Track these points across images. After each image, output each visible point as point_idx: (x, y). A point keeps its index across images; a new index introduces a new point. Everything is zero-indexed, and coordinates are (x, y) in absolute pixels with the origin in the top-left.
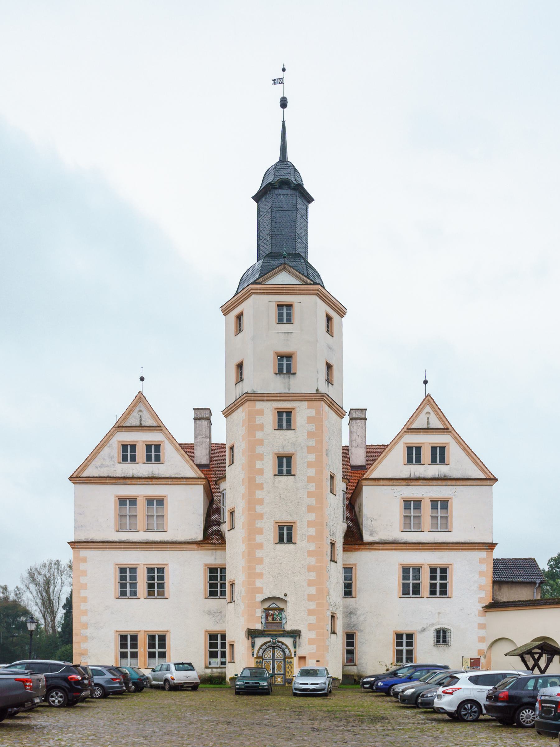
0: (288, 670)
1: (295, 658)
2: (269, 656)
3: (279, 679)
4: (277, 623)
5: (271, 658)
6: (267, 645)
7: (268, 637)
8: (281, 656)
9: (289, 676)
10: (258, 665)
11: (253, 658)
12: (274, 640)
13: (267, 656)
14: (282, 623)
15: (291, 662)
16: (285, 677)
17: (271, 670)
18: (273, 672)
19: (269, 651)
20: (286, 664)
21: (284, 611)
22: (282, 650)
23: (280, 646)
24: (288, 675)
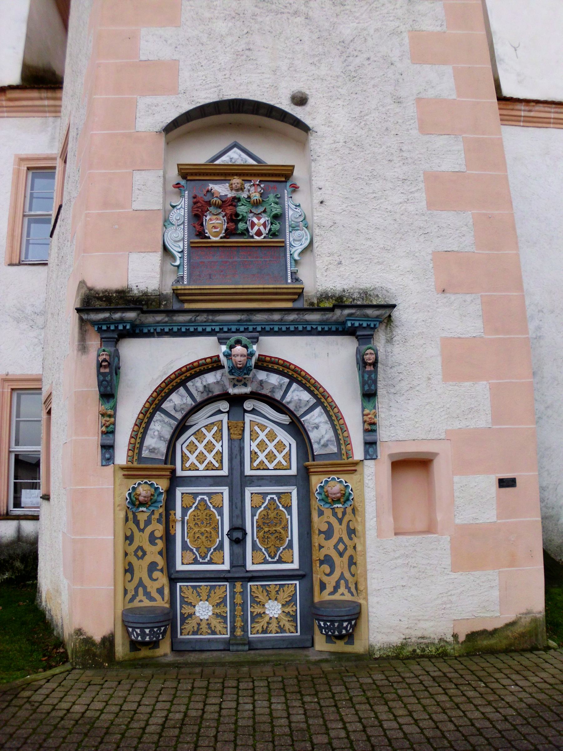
0: (329, 548)
1: (369, 467)
2: (210, 457)
4: (260, 246)
5: (225, 472)
7: (204, 333)
8: (280, 457)
9: (336, 588)
10: (142, 518)
11: (109, 469)
12: (239, 349)
13: (201, 458)
14: (282, 247)
16: (308, 592)
17: (221, 547)
19: (208, 427)
20: (315, 504)
21: (295, 188)
22: (285, 419)
23: (278, 396)
24: (331, 582)
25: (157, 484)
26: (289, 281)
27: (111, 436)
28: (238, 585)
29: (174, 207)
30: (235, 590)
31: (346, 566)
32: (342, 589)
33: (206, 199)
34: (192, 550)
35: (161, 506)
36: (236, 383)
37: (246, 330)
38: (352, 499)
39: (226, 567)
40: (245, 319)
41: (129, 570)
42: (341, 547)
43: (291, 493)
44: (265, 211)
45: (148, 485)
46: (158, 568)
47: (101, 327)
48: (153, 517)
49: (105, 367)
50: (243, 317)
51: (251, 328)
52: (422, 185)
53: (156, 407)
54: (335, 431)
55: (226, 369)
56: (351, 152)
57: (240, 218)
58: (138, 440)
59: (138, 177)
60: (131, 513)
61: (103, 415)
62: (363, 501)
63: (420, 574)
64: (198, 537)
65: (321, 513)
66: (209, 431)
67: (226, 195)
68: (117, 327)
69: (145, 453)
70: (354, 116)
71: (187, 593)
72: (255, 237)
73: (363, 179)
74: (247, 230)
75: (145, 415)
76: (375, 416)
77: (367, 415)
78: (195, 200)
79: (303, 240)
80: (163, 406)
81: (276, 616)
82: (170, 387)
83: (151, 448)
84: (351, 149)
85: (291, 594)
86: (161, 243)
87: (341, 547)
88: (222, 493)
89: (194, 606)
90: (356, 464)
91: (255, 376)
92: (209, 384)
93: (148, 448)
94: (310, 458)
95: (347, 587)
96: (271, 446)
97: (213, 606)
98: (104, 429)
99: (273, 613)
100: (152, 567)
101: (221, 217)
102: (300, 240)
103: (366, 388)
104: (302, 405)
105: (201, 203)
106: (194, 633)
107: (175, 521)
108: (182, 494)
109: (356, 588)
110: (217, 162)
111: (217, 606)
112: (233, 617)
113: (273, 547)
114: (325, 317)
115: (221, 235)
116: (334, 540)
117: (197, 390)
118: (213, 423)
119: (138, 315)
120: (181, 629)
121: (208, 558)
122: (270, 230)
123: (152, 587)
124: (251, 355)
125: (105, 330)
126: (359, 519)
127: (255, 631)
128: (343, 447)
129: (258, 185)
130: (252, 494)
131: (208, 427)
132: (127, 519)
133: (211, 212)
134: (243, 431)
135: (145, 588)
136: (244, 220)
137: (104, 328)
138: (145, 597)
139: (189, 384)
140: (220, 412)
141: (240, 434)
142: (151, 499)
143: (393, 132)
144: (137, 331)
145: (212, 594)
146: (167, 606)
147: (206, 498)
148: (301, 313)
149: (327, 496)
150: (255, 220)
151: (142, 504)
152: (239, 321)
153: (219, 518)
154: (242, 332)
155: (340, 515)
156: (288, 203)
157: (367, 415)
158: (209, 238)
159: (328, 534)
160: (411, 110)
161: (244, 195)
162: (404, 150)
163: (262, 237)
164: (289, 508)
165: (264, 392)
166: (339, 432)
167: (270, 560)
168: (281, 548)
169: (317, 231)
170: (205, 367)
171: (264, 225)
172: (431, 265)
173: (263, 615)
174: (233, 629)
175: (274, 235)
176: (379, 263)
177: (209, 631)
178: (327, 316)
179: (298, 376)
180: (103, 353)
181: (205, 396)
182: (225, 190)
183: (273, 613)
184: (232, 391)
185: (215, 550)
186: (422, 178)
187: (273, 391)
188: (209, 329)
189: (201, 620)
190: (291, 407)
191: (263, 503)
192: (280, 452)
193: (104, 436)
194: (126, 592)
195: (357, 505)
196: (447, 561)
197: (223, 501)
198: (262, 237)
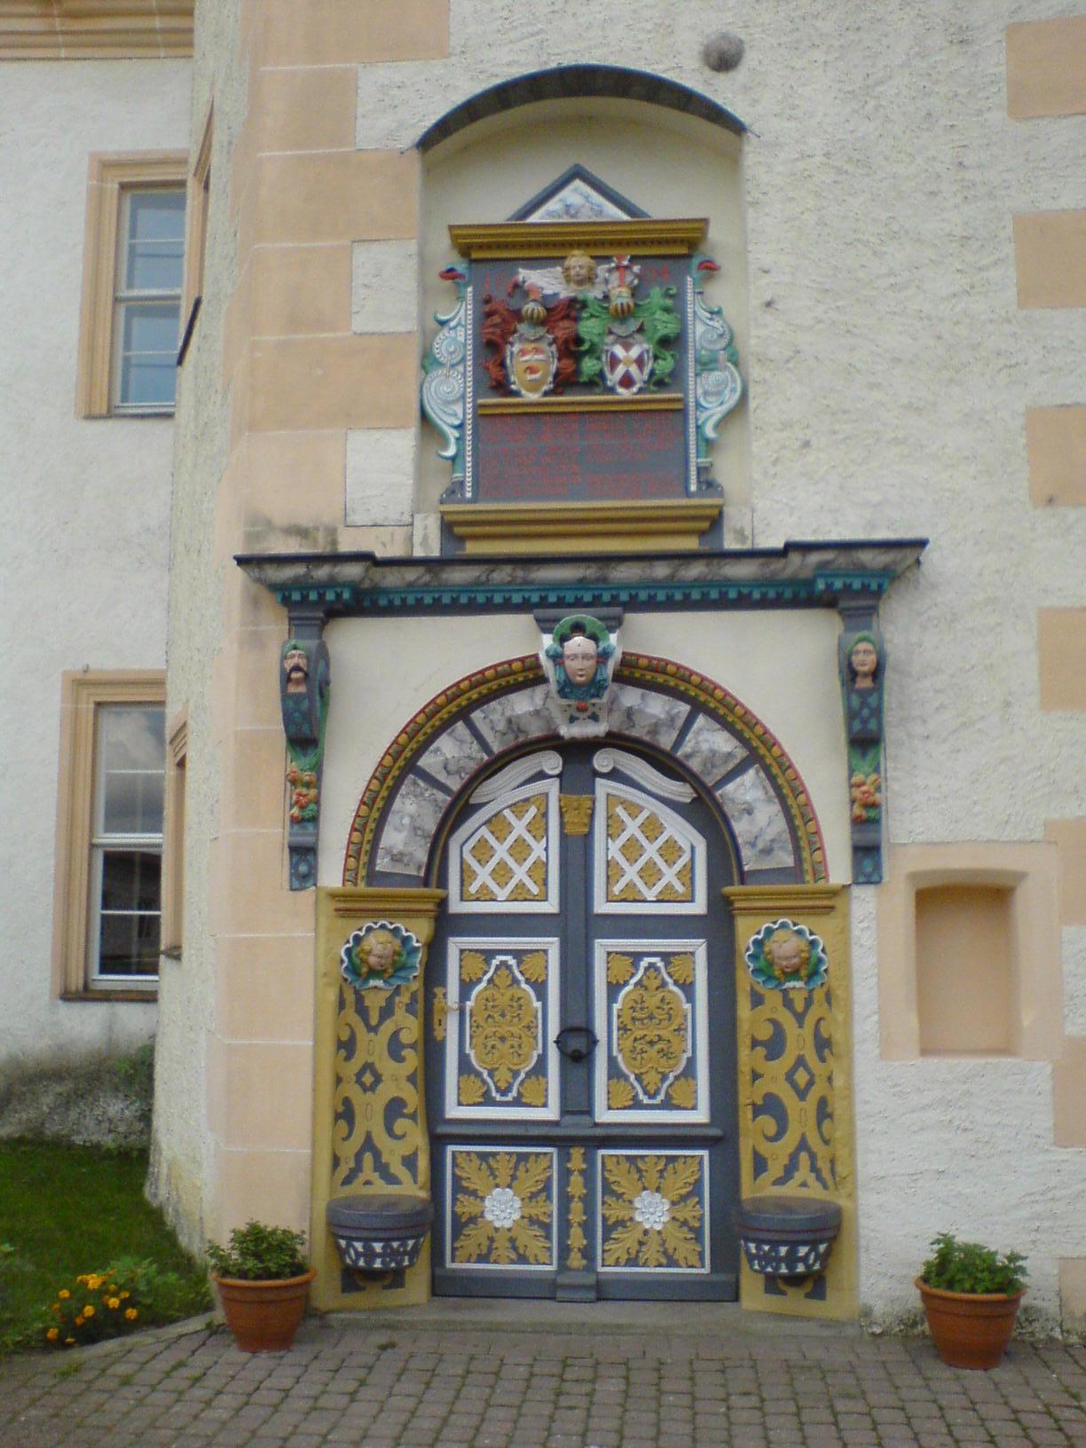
1: (864, 902)
2: (520, 873)
3: (652, 1212)
5: (551, 906)
6: (491, 719)
7: (507, 607)
8: (670, 875)
9: (790, 1169)
10: (375, 1002)
11: (308, 895)
12: (578, 643)
13: (502, 873)
15: (810, 968)
17: (540, 1068)
18: (577, 1100)
19: (519, 807)
20: (745, 979)
21: (710, 268)
22: (681, 792)
23: (666, 741)
24: (778, 1154)
25: (407, 931)
26: (693, 488)
27: (310, 827)
28: (577, 1153)
29: (443, 323)
30: (569, 1165)
31: (812, 1121)
32: (804, 1173)
33: (513, 303)
34: (478, 1074)
35: (415, 977)
36: (577, 714)
37: (596, 602)
38: (826, 971)
39: (551, 1113)
40: (593, 576)
41: (346, 1114)
42: (801, 1077)
43: (692, 954)
44: (641, 330)
45: (387, 933)
46: (405, 1111)
47: (290, 596)
48: (397, 999)
49: (298, 682)
50: (590, 572)
51: (606, 597)
52: (1008, 249)
53: (406, 765)
54: (789, 819)
55: (553, 686)
56: (839, 178)
57: (585, 347)
58: (369, 836)
59: (365, 259)
60: (352, 991)
61: (294, 782)
62: (847, 976)
63: (980, 1145)
64: (493, 1047)
65: (757, 1000)
66: (519, 817)
67: (555, 295)
68: (321, 596)
69: (383, 864)
70: (850, 89)
71: (467, 1169)
72: (620, 390)
73: (866, 244)
74: (601, 375)
75: (382, 783)
76: (878, 789)
77: (859, 785)
78: (487, 308)
79: (727, 392)
80: (422, 763)
81: (658, 1227)
82: (436, 721)
83: (395, 852)
84: (840, 171)
85: (691, 1180)
86: (415, 407)
87: (801, 1077)
88: (545, 952)
89: (483, 1199)
90: (834, 893)
91: (614, 700)
92: (518, 717)
93: (388, 852)
94: (736, 878)
95: (814, 1168)
96: (651, 851)
97: (523, 1199)
98: (295, 811)
99: (652, 1219)
100: (394, 1108)
101: (543, 345)
102: (719, 394)
103: (857, 725)
104: (718, 762)
105: (501, 315)
106: (482, 1258)
107: (444, 1011)
108: (462, 951)
109: (833, 1171)
110: (534, 218)
111: (530, 1198)
112: (565, 1225)
113: (653, 1072)
114: (767, 571)
115: (545, 388)
116: (787, 1061)
117: (492, 728)
118: (526, 800)
119: (367, 570)
120: (454, 1249)
121: (514, 1093)
122: (652, 373)
123: (392, 1152)
124: (603, 657)
125: (296, 602)
126: (840, 1017)
127: (611, 1260)
128: (806, 854)
129: (627, 267)
130: (609, 954)
131: (519, 807)
132: (341, 1004)
133: (522, 335)
134: (592, 816)
135: (377, 1154)
136: (593, 351)
137: (296, 596)
138: (377, 1174)
139: (477, 716)
140: (541, 776)
141: (585, 825)
142: (394, 962)
143: (945, 122)
144: (367, 603)
145: (521, 1173)
146: (424, 1194)
147: (512, 961)
148: (715, 562)
149: (771, 964)
150: (619, 351)
151: (374, 973)
152: (581, 580)
153: (538, 1005)
154: (587, 605)
155: (799, 1006)
156: (693, 305)
157: (859, 785)
158: (516, 394)
159: (774, 1047)
160: (994, 60)
161: (594, 293)
162: (966, 163)
163: (635, 389)
164: (688, 988)
165: (635, 733)
166: (798, 822)
167: (646, 1101)
168: (671, 1076)
169: (755, 372)
170: (511, 679)
171: (640, 362)
172: (1023, 441)
173: (628, 1224)
174: (564, 1251)
175: (660, 384)
176: (896, 441)
177: (513, 1256)
178: (772, 567)
179: (709, 699)
180: (294, 652)
181: (511, 741)
182: (554, 281)
183: (652, 1219)
184: (567, 731)
185: (528, 1075)
186: (1009, 231)
187: (655, 729)
188: (516, 598)
189: (497, 1230)
190: (695, 765)
191: (633, 975)
192: (670, 863)
193: (296, 827)
194: (336, 1162)
195: (834, 984)
196: (1044, 1121)
197: (546, 968)
198: (635, 389)
